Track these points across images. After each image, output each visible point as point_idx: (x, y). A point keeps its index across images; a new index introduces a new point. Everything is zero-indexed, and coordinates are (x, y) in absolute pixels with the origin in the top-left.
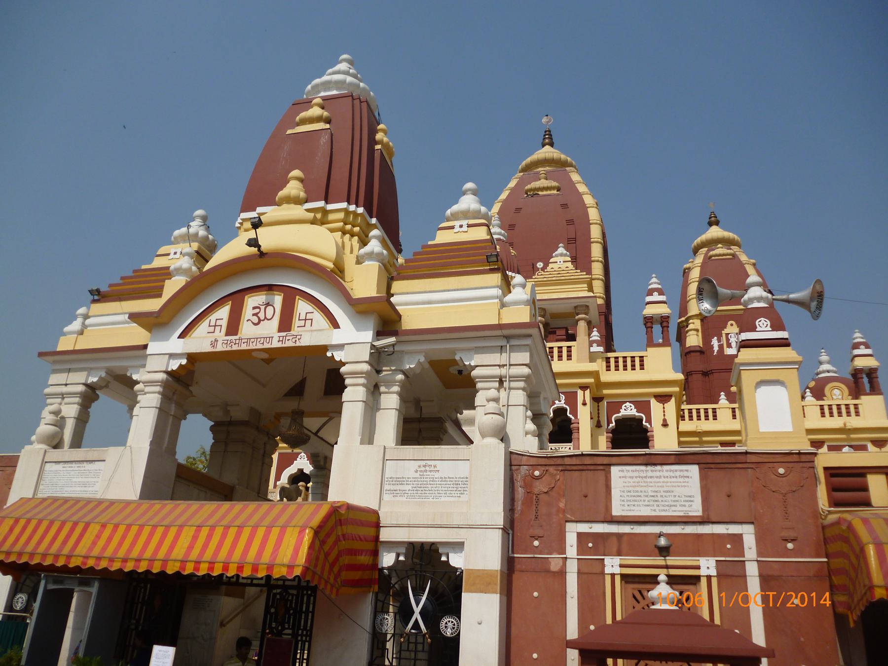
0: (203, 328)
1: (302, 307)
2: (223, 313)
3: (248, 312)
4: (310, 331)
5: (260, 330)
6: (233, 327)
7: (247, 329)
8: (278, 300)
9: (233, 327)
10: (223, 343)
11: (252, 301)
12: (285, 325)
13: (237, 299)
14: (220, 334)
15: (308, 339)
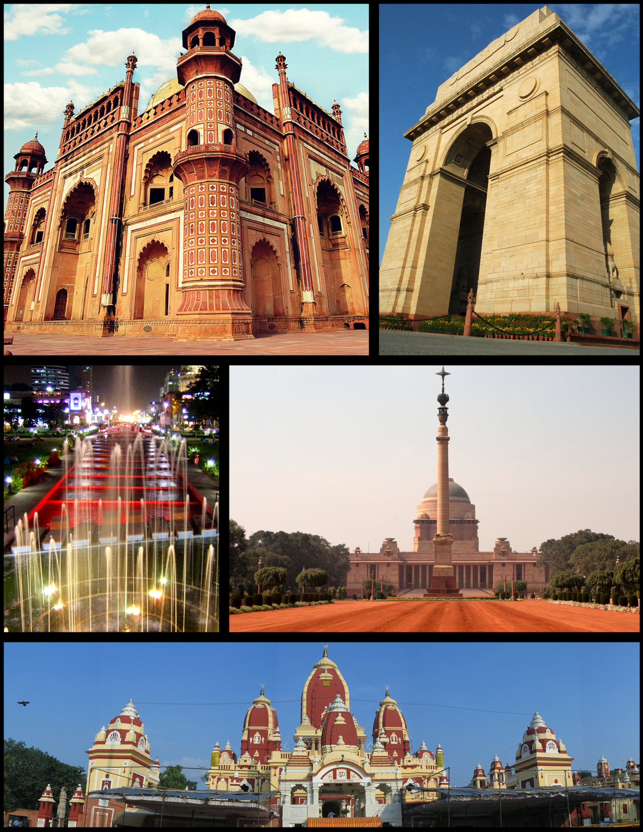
0: (326, 777)
1: (352, 773)
2: (331, 773)
3: (338, 774)
4: (355, 779)
5: (342, 779)
6: (335, 777)
7: (338, 778)
8: (345, 771)
9: (335, 777)
10: (333, 781)
11: (338, 771)
12: (348, 777)
13: (334, 770)
14: (332, 778)
15: (355, 782)
